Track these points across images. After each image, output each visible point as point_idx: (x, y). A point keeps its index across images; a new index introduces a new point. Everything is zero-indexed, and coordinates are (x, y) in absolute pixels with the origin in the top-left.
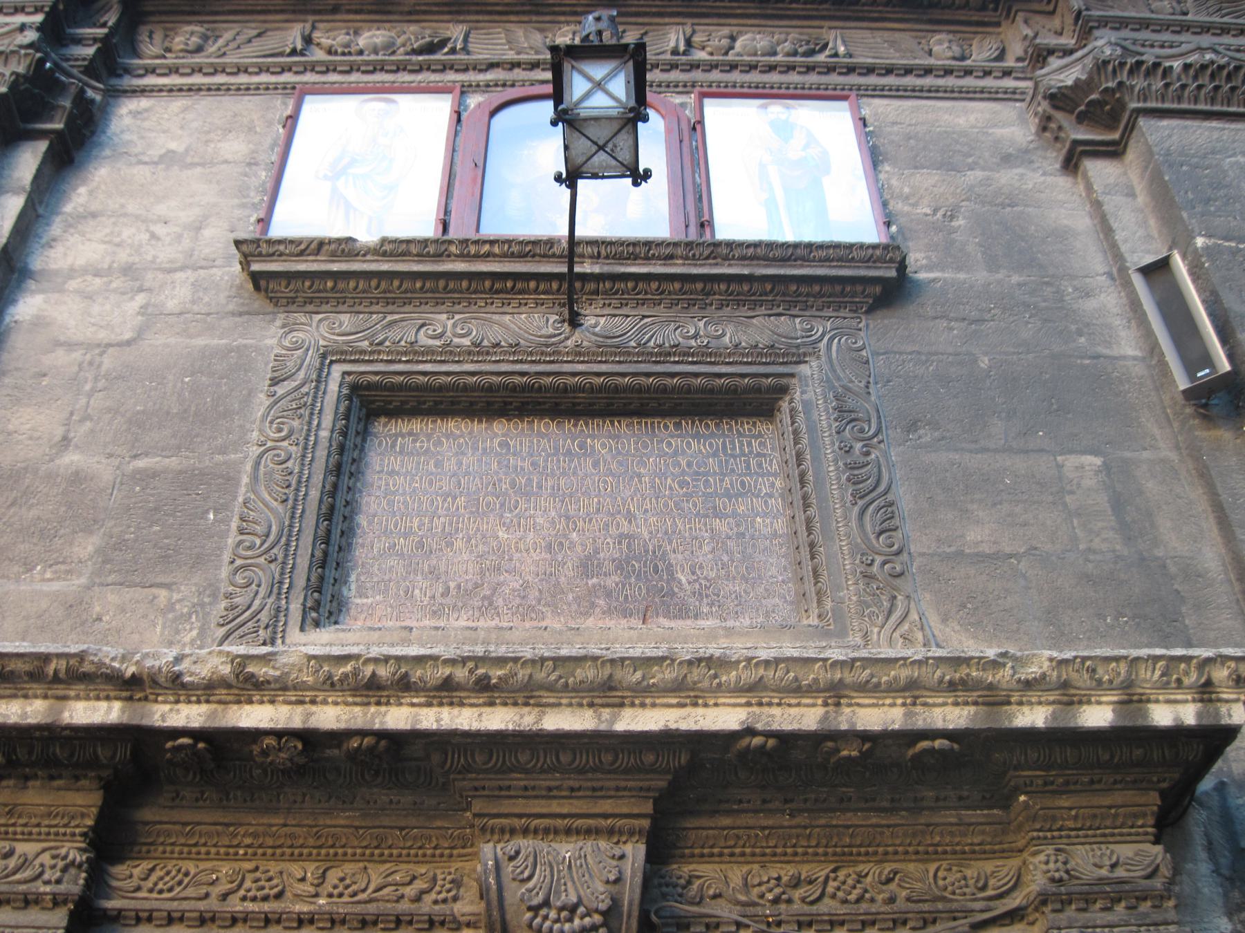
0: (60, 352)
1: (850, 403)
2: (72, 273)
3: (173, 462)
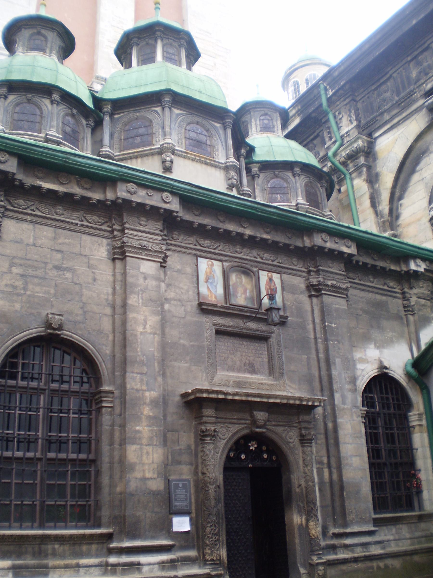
3: (196, 344)
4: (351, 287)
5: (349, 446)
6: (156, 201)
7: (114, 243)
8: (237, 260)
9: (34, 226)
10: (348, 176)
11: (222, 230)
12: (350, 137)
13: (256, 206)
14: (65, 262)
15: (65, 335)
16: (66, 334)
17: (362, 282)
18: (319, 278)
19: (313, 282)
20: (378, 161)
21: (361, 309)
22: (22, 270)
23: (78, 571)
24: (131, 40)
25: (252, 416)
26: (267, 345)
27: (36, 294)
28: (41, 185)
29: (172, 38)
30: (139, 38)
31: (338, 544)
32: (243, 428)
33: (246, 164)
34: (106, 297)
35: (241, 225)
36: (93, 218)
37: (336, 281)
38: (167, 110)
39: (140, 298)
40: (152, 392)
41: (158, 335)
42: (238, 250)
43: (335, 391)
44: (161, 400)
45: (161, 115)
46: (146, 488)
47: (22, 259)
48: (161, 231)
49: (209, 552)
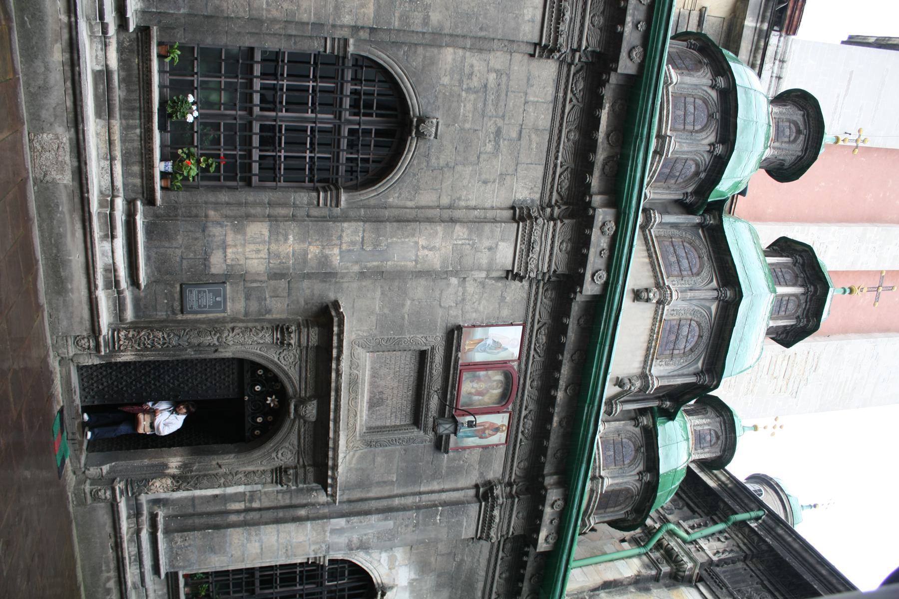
0: (439, 292)
1: (411, 441)
2: (464, 288)
4: (493, 544)
5: (274, 539)
6: (594, 262)
7: (535, 209)
8: (522, 381)
9: (551, 102)
10: (643, 550)
11: (560, 358)
13: (596, 403)
14: (506, 142)
15: (411, 143)
16: (412, 144)
17: (499, 562)
18: (503, 498)
19: (497, 489)
20: (666, 590)
21: (462, 560)
22: (493, 86)
23: (106, 159)
24: (801, 256)
25: (310, 399)
26: (408, 425)
27: (462, 105)
29: (808, 306)
30: (803, 265)
31: (142, 521)
32: (295, 386)
33: (651, 408)
34: (463, 198)
35: (569, 385)
36: (566, 181)
37: (500, 522)
38: (715, 294)
39: (463, 241)
40: (338, 258)
41: (415, 267)
43: (348, 518)
44: (328, 270)
46: (213, 250)
47: (508, 86)
48: (555, 271)
49: (130, 335)
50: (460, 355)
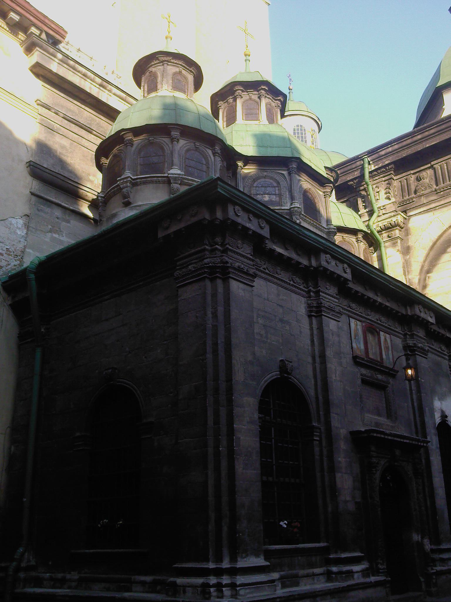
7: (309, 302)
8: (369, 321)
9: (266, 282)
12: (386, 211)
14: (285, 316)
18: (414, 341)
20: (410, 236)
28: (275, 249)
30: (243, 91)
42: (369, 313)
45: (288, 180)
50: (366, 359)
